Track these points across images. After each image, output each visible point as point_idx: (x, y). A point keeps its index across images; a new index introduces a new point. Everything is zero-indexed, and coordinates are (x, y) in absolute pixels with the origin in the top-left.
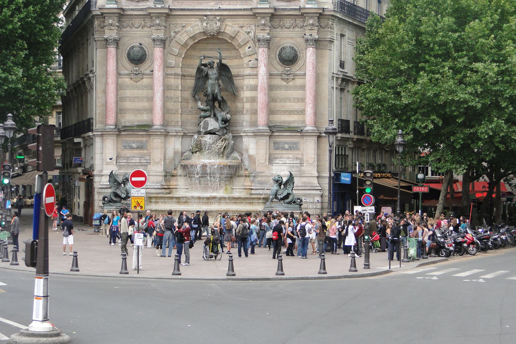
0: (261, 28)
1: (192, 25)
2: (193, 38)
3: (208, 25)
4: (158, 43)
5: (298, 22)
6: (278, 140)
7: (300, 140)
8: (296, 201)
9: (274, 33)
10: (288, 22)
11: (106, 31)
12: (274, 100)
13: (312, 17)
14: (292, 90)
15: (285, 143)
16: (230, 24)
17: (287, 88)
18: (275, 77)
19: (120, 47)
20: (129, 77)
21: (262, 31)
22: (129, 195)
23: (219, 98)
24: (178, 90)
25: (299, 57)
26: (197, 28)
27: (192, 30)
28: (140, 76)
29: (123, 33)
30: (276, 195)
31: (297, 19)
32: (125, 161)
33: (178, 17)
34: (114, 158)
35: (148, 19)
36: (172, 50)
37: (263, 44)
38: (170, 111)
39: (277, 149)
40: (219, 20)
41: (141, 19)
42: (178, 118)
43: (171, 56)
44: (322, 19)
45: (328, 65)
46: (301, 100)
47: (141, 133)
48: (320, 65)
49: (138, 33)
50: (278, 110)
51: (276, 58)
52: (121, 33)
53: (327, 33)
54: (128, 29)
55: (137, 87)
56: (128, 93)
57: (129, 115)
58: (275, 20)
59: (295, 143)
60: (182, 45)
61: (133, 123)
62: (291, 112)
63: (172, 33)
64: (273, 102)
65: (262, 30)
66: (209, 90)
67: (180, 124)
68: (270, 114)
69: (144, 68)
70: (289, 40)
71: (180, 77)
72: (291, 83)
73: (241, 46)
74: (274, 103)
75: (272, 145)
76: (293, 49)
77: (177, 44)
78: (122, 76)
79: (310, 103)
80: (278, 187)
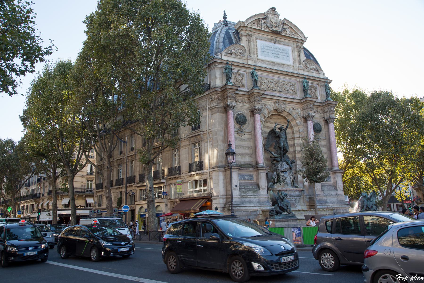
20: (237, 132)
26: (272, 107)
34: (238, 185)
35: (245, 98)
41: (241, 98)
55: (241, 140)
66: (282, 144)
69: (245, 127)
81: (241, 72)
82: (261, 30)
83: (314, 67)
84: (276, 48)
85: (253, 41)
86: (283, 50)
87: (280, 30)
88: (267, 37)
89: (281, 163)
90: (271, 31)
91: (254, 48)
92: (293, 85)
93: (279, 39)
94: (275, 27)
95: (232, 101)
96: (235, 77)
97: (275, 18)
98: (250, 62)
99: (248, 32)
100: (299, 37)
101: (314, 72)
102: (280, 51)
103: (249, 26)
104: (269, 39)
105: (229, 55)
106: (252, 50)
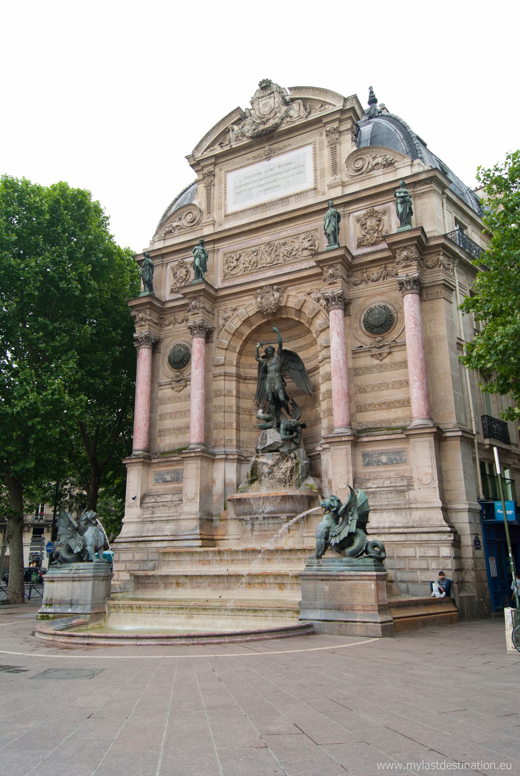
0: (329, 282)
1: (245, 306)
2: (247, 322)
3: (263, 300)
4: (195, 332)
5: (389, 269)
6: (369, 449)
7: (407, 446)
8: (370, 549)
9: (355, 292)
10: (375, 273)
11: (136, 329)
12: (362, 389)
13: (405, 248)
14: (389, 370)
15: (381, 454)
16: (293, 293)
17: (381, 368)
18: (361, 355)
19: (162, 351)
21: (331, 286)
22: (87, 548)
23: (281, 397)
24: (232, 396)
25: (396, 319)
26: (251, 308)
27: (244, 311)
28: (183, 383)
29: (165, 332)
30: (326, 538)
31: (387, 265)
32: (153, 500)
33: (227, 298)
36: (220, 343)
37: (334, 303)
38: (218, 425)
39: (368, 464)
40: (277, 290)
42: (232, 434)
43: (220, 351)
44: (428, 257)
45: (445, 322)
46: (405, 384)
47: (175, 459)
48: (432, 325)
49: (182, 329)
50: (370, 405)
51: (360, 326)
52: (163, 333)
53: (437, 274)
54: (171, 327)
56: (169, 408)
57: (170, 437)
58: (356, 273)
59: (398, 452)
60: (233, 335)
61: (174, 447)
62: (389, 405)
63: (220, 321)
64: (361, 393)
65: (330, 284)
66: (267, 386)
67: (235, 443)
68: (358, 412)
70: (379, 298)
71: (235, 378)
72: (387, 360)
73: (311, 321)
74: (363, 395)
75: (360, 458)
76: (384, 309)
77: (227, 334)
78: (163, 387)
79: (416, 381)
80: (331, 520)
81: (185, 260)
82: (232, 152)
83: (379, 160)
84: (271, 170)
85: (220, 182)
86: (287, 164)
87: (277, 120)
88: (250, 155)
89: (263, 434)
90: (251, 137)
91: (220, 197)
92: (310, 236)
93: (281, 145)
94: (264, 123)
95: (143, 327)
96: (174, 275)
97: (271, 102)
98: (207, 231)
99: (205, 171)
100: (331, 106)
101: (381, 171)
102: (282, 169)
103: (208, 154)
104: (258, 156)
105: (168, 236)
106: (215, 202)
